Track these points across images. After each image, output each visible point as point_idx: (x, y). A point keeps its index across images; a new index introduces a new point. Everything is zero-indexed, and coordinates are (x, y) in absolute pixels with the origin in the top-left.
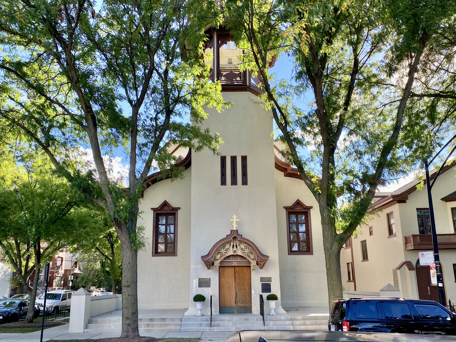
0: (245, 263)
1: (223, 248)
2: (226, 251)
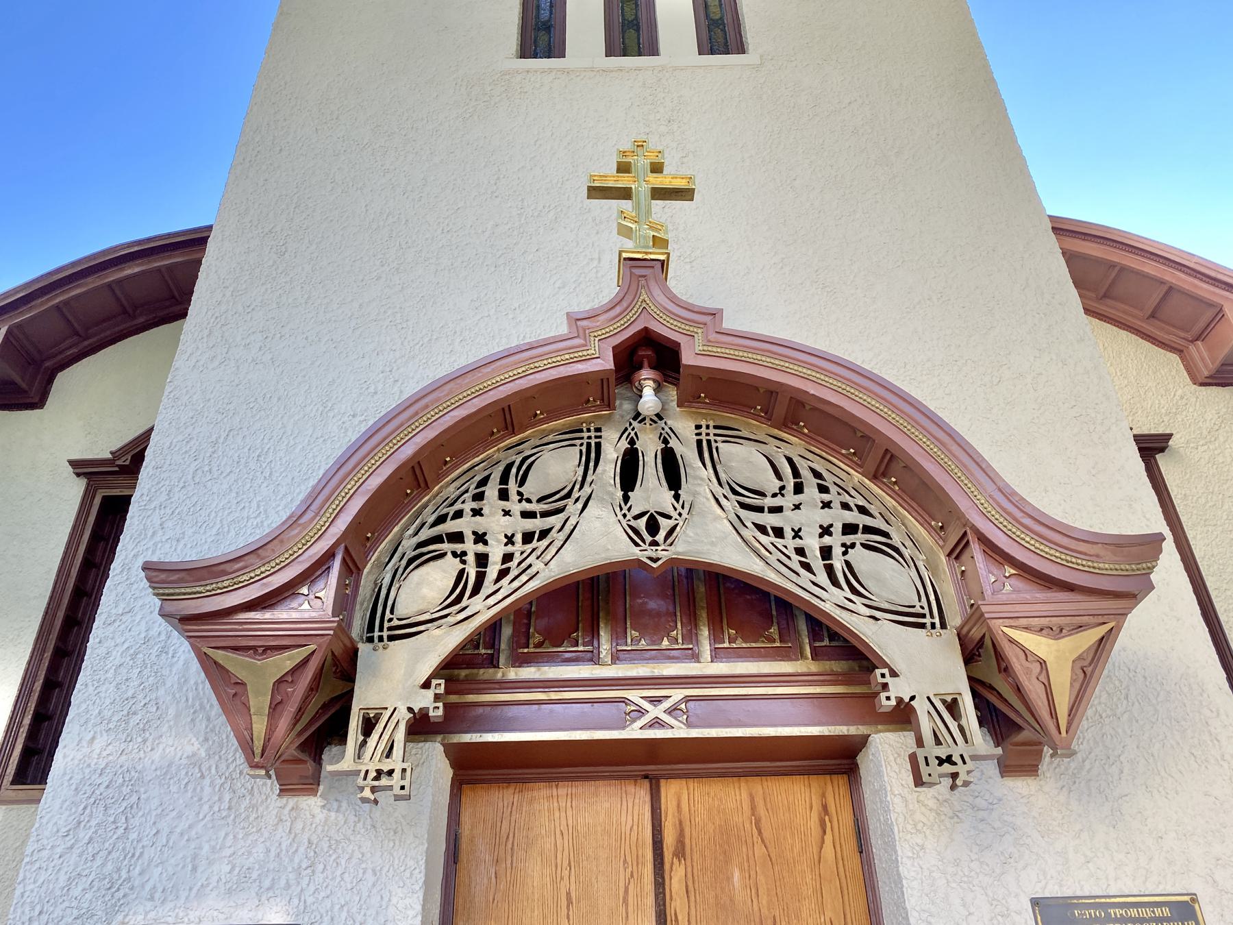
1: (492, 491)
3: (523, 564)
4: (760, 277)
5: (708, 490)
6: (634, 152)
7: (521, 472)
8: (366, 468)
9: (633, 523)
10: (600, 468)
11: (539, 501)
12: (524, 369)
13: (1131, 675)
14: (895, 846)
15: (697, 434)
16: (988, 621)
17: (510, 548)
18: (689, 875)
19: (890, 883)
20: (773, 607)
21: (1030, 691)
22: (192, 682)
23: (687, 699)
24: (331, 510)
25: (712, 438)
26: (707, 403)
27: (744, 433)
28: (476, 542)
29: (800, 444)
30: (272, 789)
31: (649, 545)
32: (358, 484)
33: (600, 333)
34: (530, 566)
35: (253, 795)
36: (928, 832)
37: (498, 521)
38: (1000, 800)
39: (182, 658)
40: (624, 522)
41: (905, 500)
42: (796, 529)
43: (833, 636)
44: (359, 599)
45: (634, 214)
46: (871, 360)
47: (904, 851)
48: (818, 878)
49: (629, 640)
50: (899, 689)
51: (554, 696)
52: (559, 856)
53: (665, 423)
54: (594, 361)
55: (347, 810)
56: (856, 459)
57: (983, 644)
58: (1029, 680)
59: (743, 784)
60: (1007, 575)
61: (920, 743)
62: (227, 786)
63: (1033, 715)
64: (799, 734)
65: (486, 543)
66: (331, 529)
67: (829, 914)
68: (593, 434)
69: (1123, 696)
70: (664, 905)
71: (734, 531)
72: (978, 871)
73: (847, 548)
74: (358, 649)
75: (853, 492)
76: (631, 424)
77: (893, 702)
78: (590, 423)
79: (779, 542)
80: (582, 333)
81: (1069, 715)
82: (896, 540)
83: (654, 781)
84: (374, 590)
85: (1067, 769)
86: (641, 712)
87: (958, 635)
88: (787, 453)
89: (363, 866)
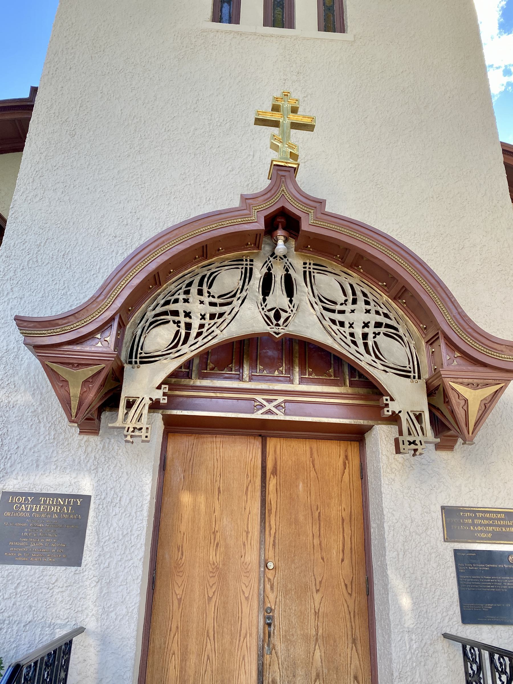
0: (335, 409)
1: (194, 290)
2: (217, 310)
3: (209, 331)
4: (342, 175)
5: (307, 299)
6: (282, 99)
7: (210, 281)
8: (131, 274)
9: (267, 313)
10: (251, 282)
11: (219, 297)
12: (216, 225)
13: (505, 406)
14: (381, 478)
15: (304, 268)
16: (443, 378)
17: (203, 321)
18: (278, 483)
19: (376, 494)
20: (332, 359)
21: (458, 413)
22: (32, 374)
23: (285, 401)
24: (113, 296)
25: (312, 270)
26: (311, 251)
27: (329, 269)
28: (185, 317)
29: (357, 277)
30: (75, 431)
31: (275, 326)
32: (127, 282)
33: (258, 207)
34: (213, 331)
35: (66, 433)
36: (397, 473)
37: (197, 306)
38: (433, 461)
39: (27, 361)
40: (263, 312)
41: (408, 312)
42: (351, 323)
43: (361, 375)
44: (125, 341)
45: (280, 137)
46: (397, 230)
47: (384, 481)
48: (340, 489)
49: (258, 371)
50: (394, 407)
51: (219, 395)
52: (215, 470)
53: (288, 260)
54: (254, 224)
55: (113, 443)
56: (386, 288)
57: (438, 389)
58: (459, 408)
59: (307, 442)
60: (456, 356)
61: (401, 433)
62: (53, 428)
63: (458, 425)
64: (339, 422)
65: (190, 317)
66: (113, 305)
67: (344, 506)
68: (248, 263)
69: (499, 416)
70: (265, 496)
71: (319, 322)
72: (419, 492)
73: (376, 334)
74: (124, 367)
75: (382, 306)
76: (269, 259)
77: (390, 413)
78: (247, 257)
79: (342, 329)
80: (249, 207)
81: (475, 426)
82: (401, 332)
83: (264, 438)
84: (132, 337)
85: (467, 448)
86: (262, 406)
87: (426, 383)
88: (350, 282)
89: (122, 470)
